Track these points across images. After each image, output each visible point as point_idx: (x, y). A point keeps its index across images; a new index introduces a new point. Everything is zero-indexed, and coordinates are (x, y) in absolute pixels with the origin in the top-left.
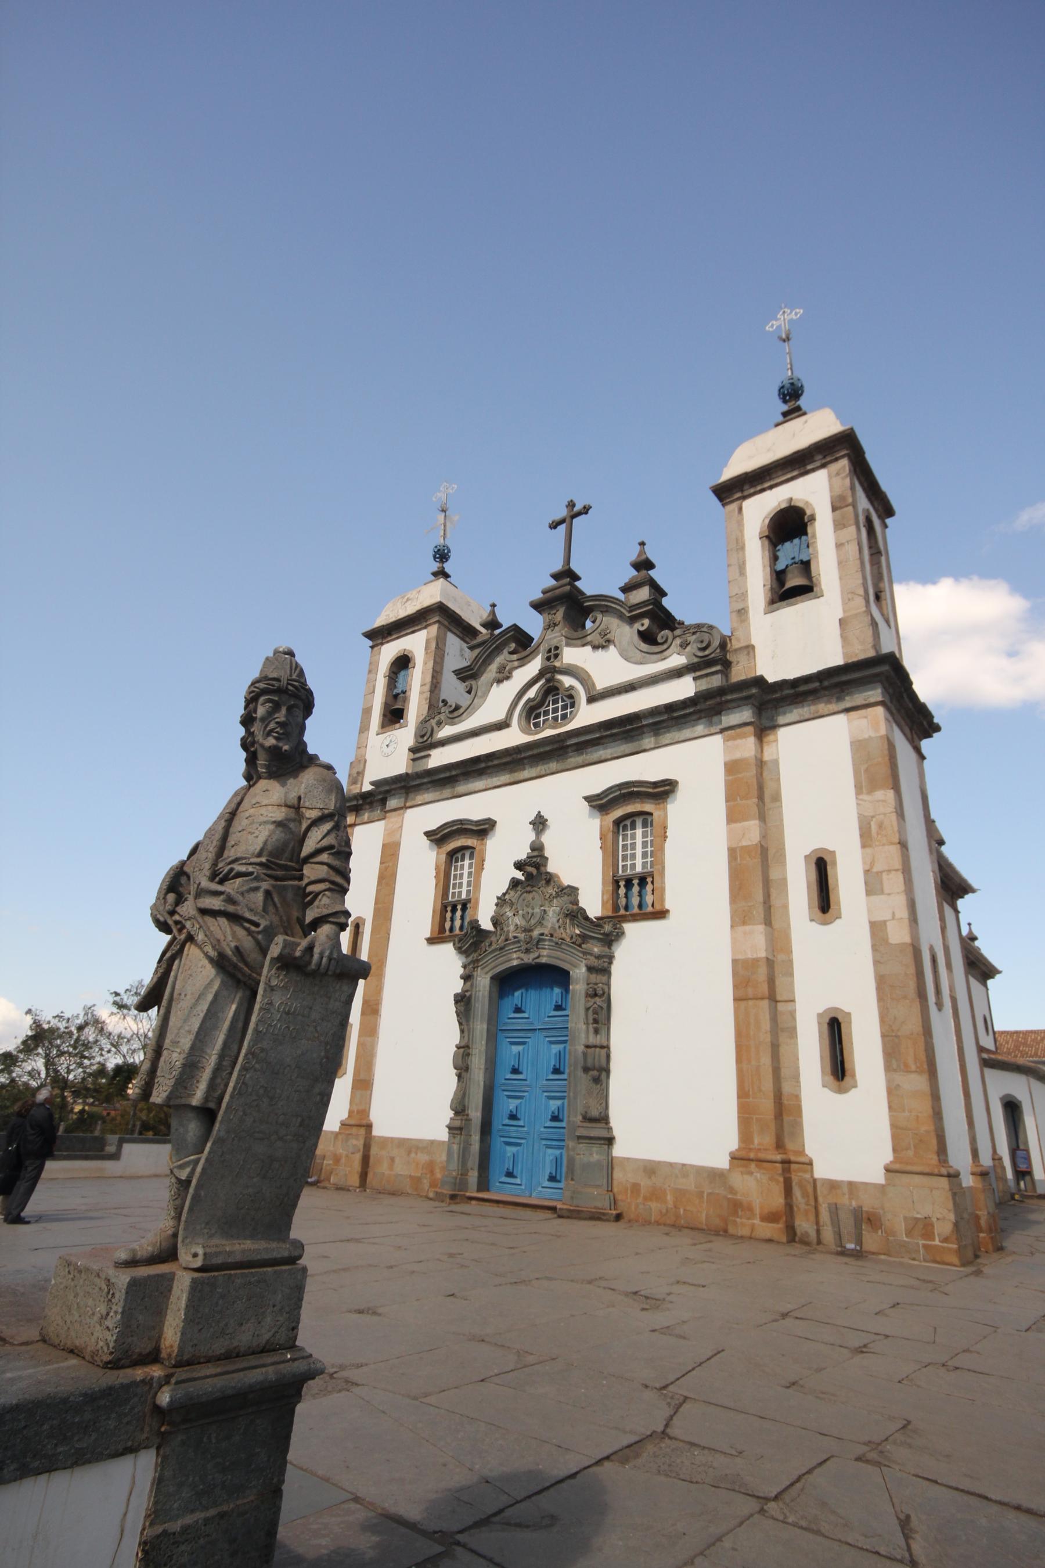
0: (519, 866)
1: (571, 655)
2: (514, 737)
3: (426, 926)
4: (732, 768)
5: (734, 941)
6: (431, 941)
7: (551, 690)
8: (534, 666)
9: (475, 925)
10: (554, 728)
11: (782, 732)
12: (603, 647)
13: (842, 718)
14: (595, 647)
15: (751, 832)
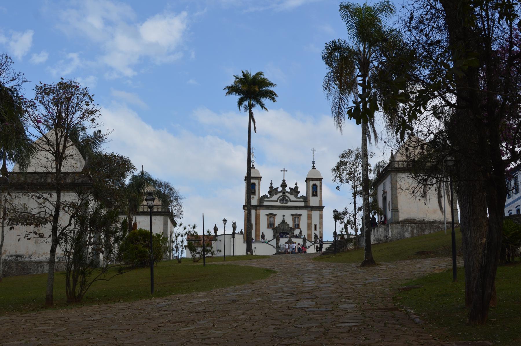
0: (283, 221)
1: (287, 194)
2: (278, 204)
3: (267, 227)
4: (308, 214)
5: (308, 232)
6: (267, 228)
7: (284, 198)
8: (281, 194)
9: (276, 227)
10: (285, 204)
11: (313, 211)
12: (292, 195)
13: (319, 211)
14: (291, 194)
15: (310, 221)
